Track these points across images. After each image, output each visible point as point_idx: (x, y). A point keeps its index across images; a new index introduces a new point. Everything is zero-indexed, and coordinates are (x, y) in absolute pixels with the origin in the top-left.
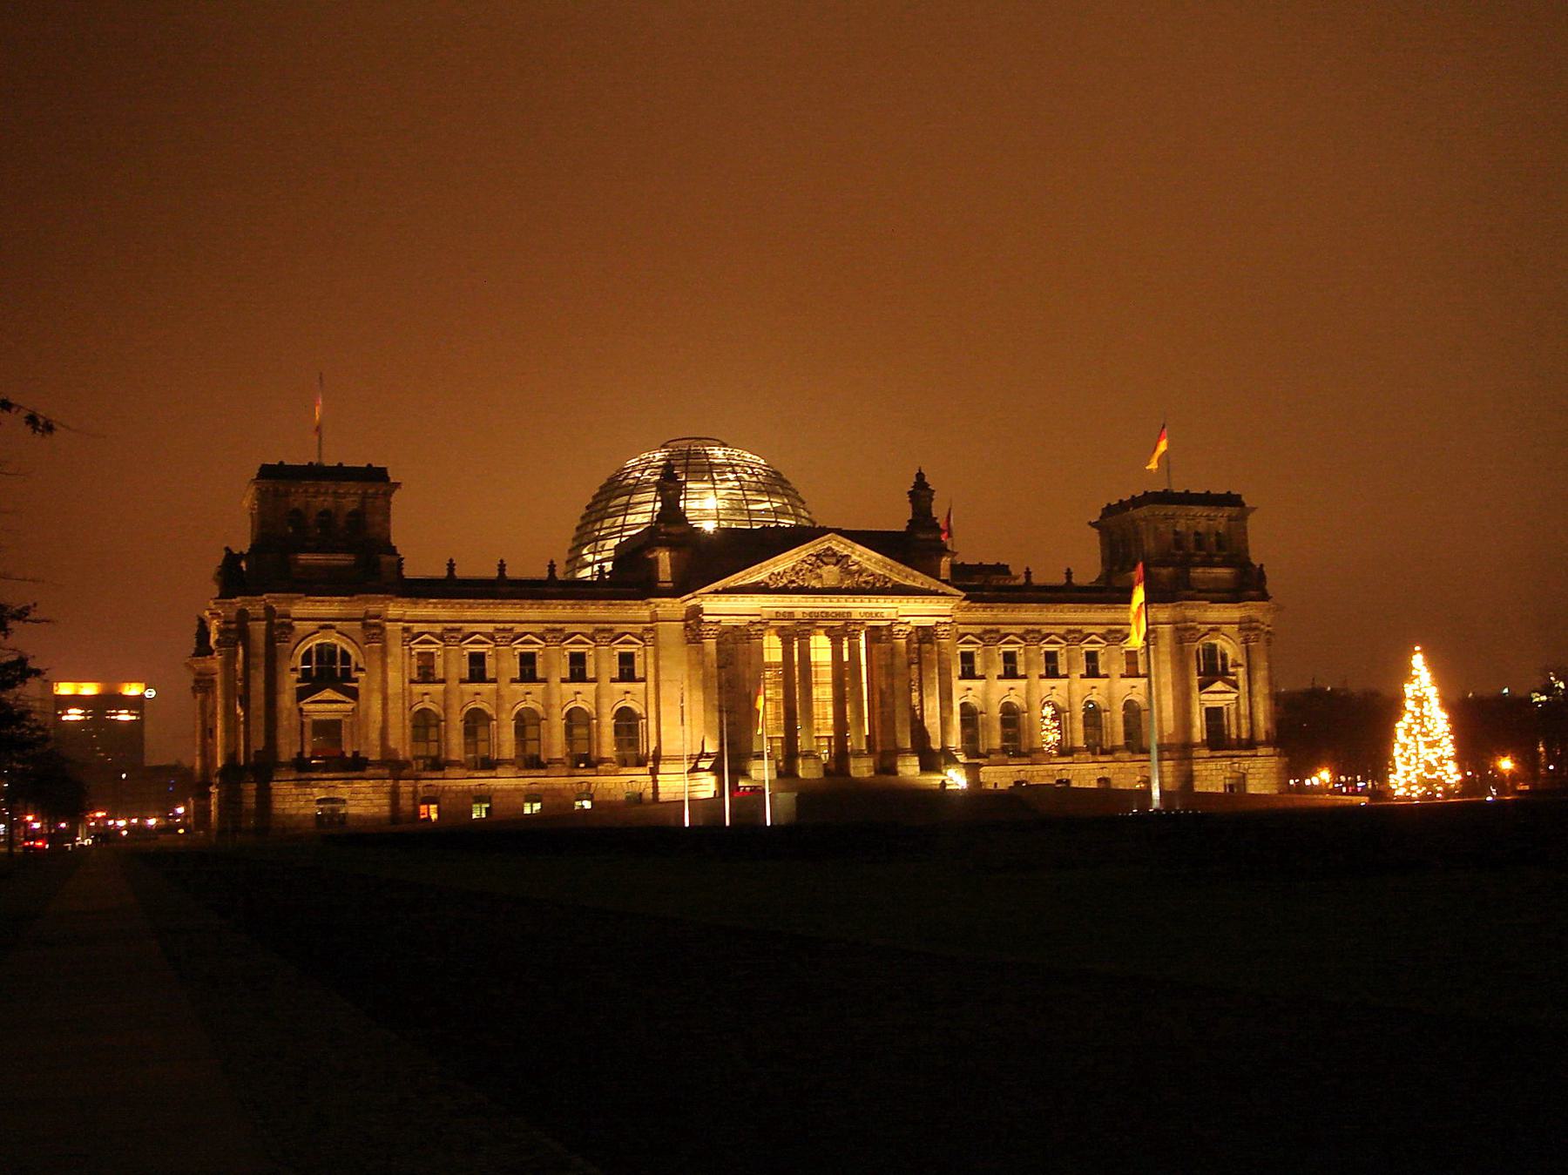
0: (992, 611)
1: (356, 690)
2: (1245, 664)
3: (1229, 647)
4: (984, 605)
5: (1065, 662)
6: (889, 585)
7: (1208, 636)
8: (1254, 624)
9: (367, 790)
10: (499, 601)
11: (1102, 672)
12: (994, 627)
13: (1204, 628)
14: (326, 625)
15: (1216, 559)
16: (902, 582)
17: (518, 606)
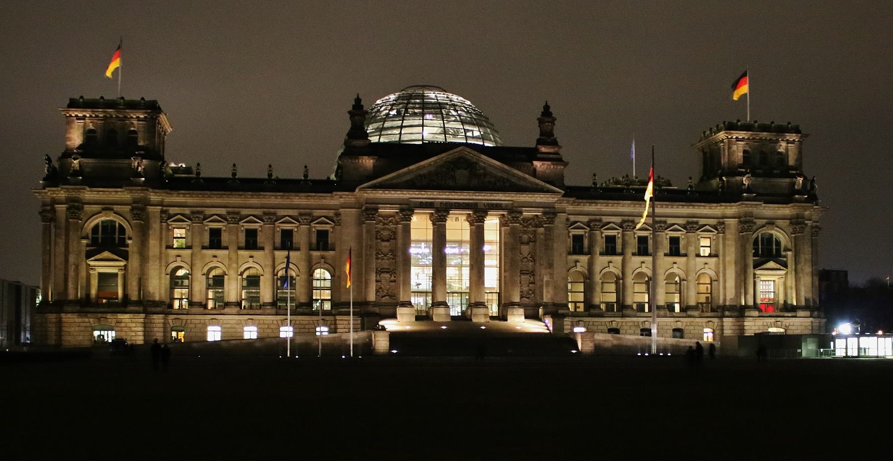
0: (596, 206)
1: (127, 252)
2: (793, 250)
3: (781, 236)
4: (589, 201)
6: (507, 184)
7: (764, 228)
8: (800, 220)
9: (127, 320)
10: (228, 193)
11: (682, 251)
12: (598, 217)
13: (760, 222)
14: (107, 207)
16: (518, 183)
17: (243, 196)
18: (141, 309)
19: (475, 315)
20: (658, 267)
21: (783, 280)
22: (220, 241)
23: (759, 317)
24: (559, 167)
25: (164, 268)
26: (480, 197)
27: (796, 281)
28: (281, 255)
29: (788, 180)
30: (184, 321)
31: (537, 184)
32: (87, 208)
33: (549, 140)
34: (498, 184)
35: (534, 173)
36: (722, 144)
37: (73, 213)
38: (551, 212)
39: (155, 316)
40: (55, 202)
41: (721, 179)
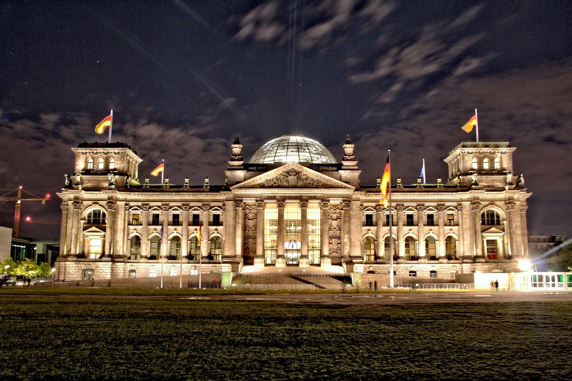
1: (106, 227)
2: (508, 220)
3: (500, 211)
4: (375, 193)
5: (417, 219)
6: (320, 184)
11: (435, 223)
14: (96, 202)
18: (110, 259)
19: (301, 263)
20: (420, 233)
21: (502, 239)
23: (486, 262)
24: (355, 174)
25: (126, 236)
26: (303, 192)
27: (510, 240)
28: (192, 228)
29: (502, 176)
30: (136, 268)
31: (339, 184)
33: (350, 158)
34: (314, 184)
36: (459, 157)
37: (75, 205)
38: (348, 201)
39: (119, 264)
41: (459, 178)
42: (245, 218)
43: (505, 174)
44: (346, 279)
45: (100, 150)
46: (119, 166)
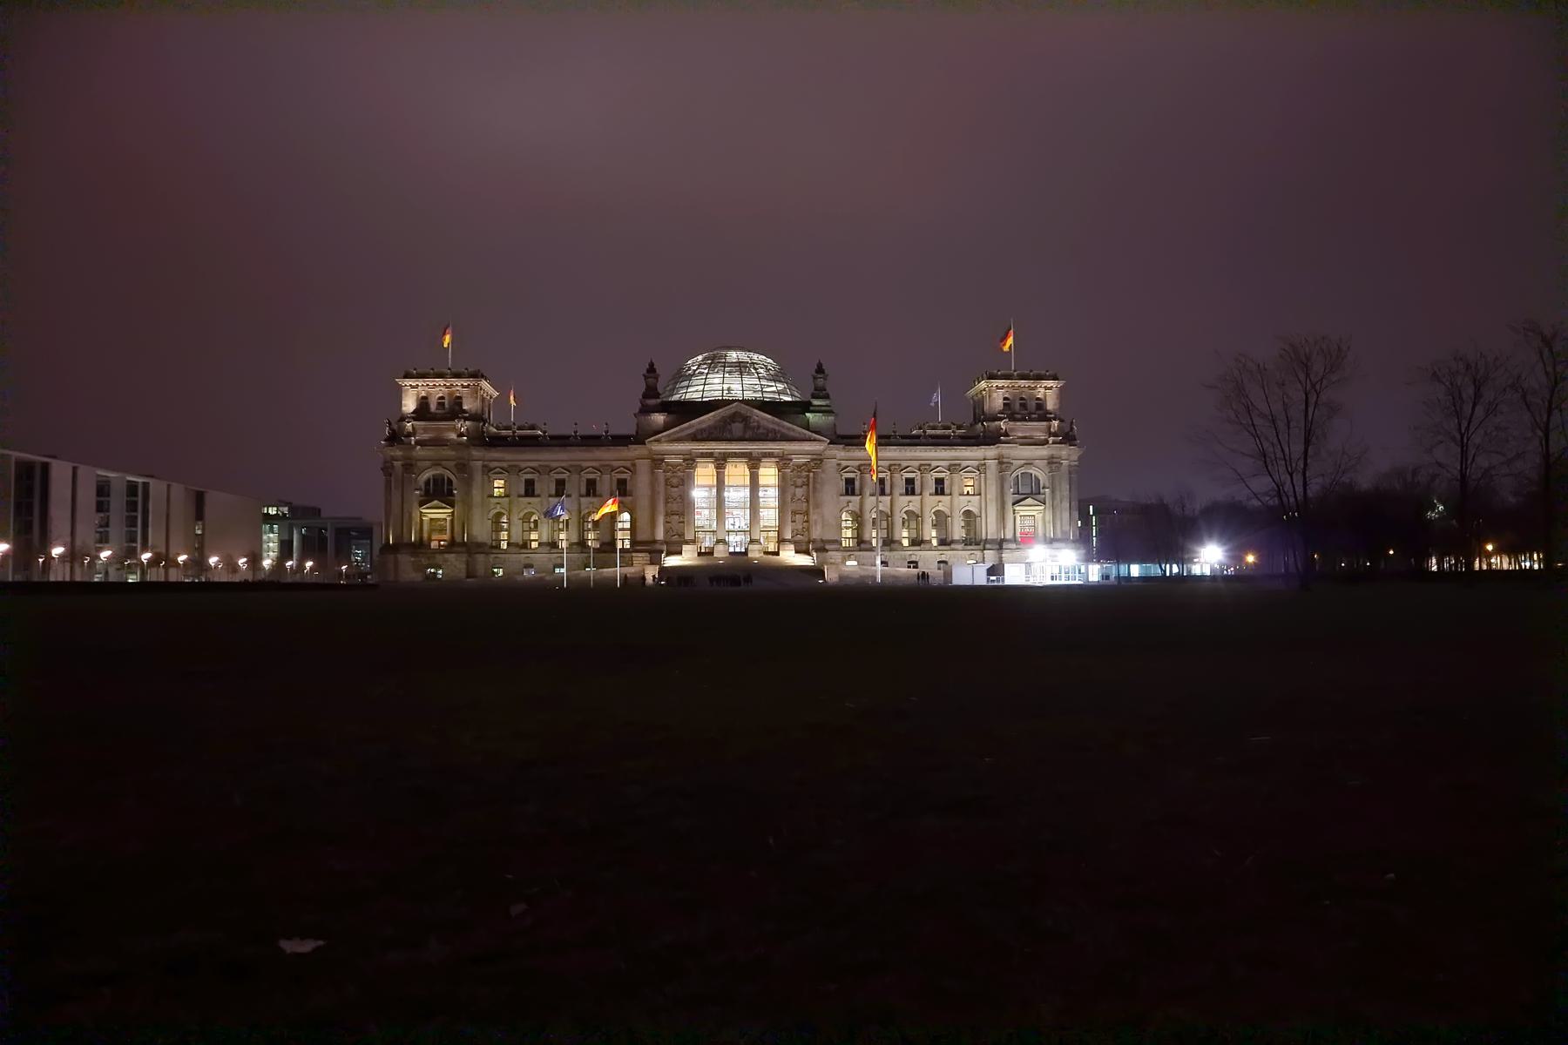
1: (454, 501)
3: (1040, 474)
11: (947, 491)
15: (1034, 416)
18: (464, 549)
21: (1041, 515)
22: (533, 491)
24: (830, 418)
29: (1045, 423)
31: (805, 434)
32: (419, 464)
34: (770, 435)
35: (807, 426)
38: (818, 461)
39: (478, 556)
40: (394, 459)
41: (983, 424)
42: (666, 485)
43: (1049, 420)
44: (817, 572)
45: (440, 381)
46: (470, 406)
